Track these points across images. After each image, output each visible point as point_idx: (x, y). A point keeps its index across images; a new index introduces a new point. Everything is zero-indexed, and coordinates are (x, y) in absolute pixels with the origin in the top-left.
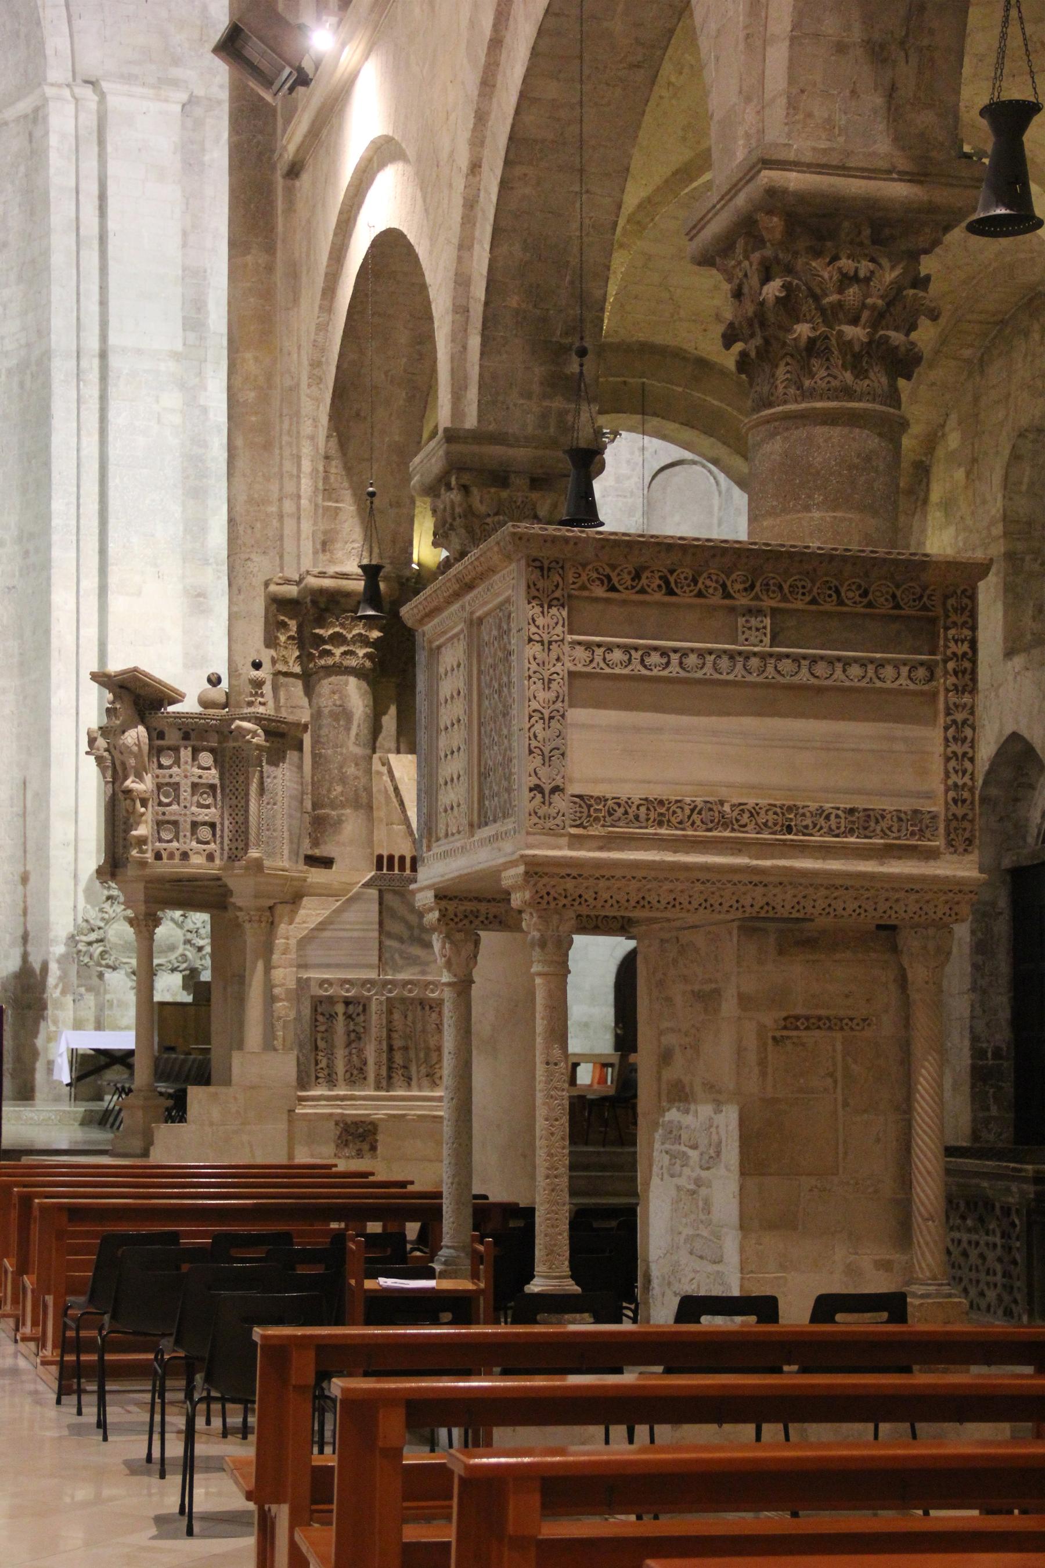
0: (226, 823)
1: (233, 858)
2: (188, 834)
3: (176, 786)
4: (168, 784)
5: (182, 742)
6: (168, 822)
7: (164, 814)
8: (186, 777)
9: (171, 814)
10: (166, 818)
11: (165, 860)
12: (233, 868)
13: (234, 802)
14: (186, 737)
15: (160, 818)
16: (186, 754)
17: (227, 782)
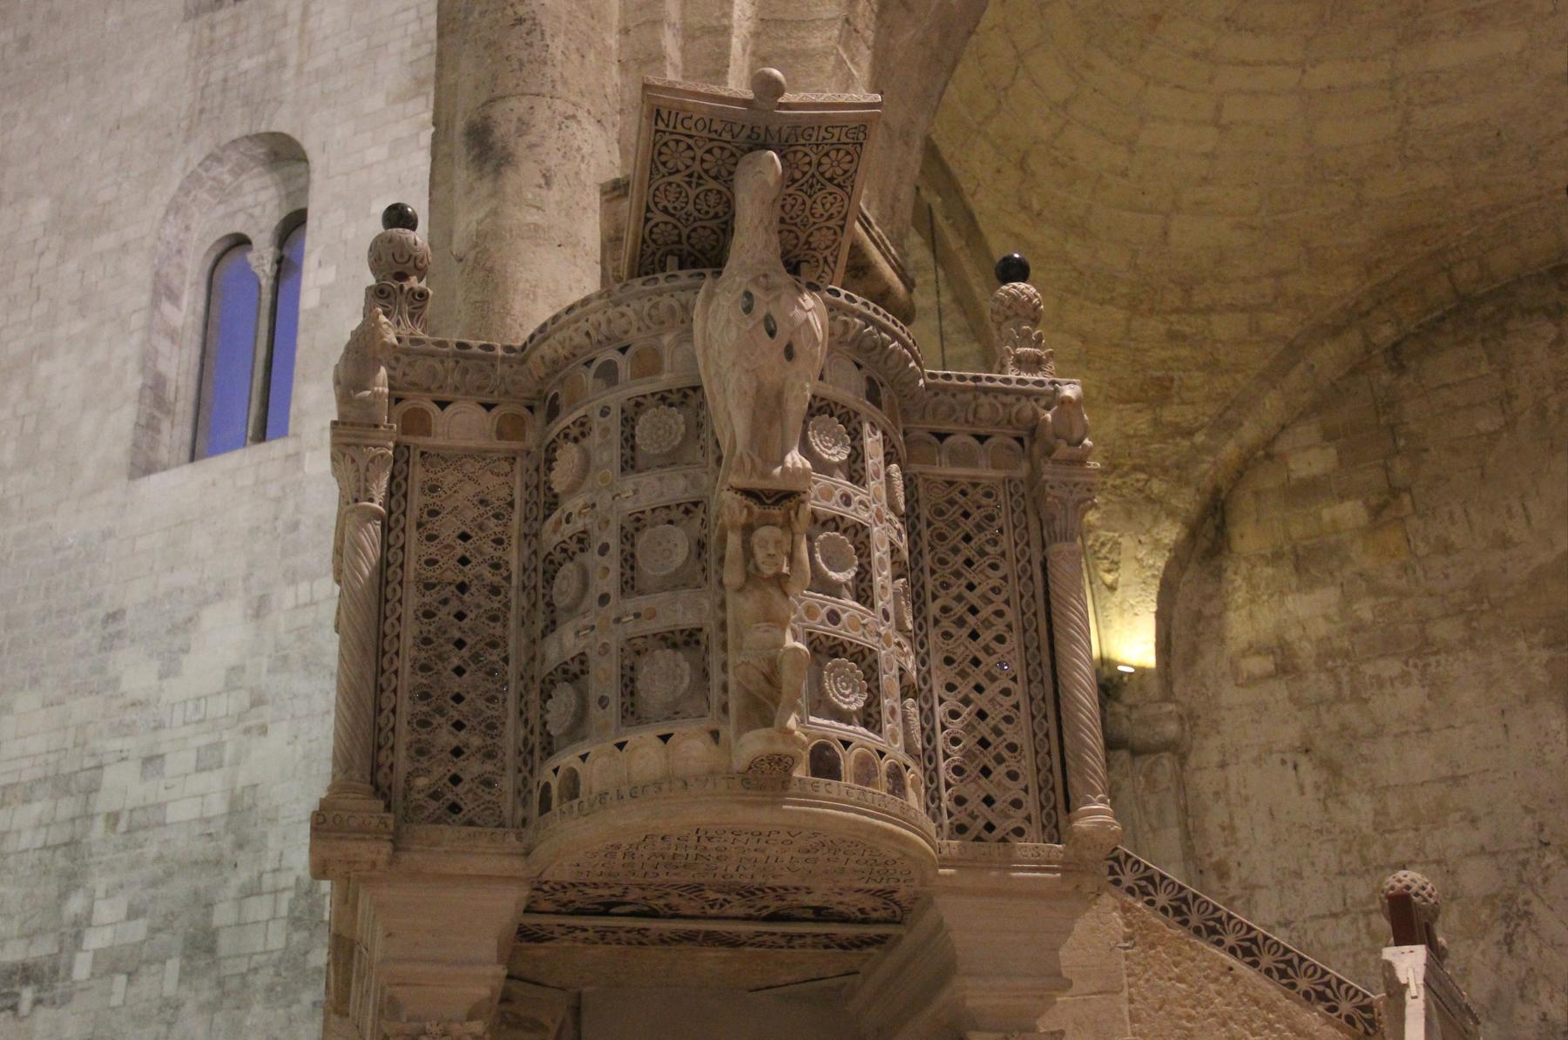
0: (940, 711)
1: (976, 829)
2: (897, 706)
3: (859, 535)
4: (835, 522)
5: (865, 407)
6: (836, 649)
7: (834, 617)
8: (879, 516)
9: (855, 624)
10: (842, 632)
11: (848, 781)
12: (1008, 863)
13: (963, 648)
14: (873, 395)
15: (823, 628)
16: (873, 443)
17: (930, 584)
